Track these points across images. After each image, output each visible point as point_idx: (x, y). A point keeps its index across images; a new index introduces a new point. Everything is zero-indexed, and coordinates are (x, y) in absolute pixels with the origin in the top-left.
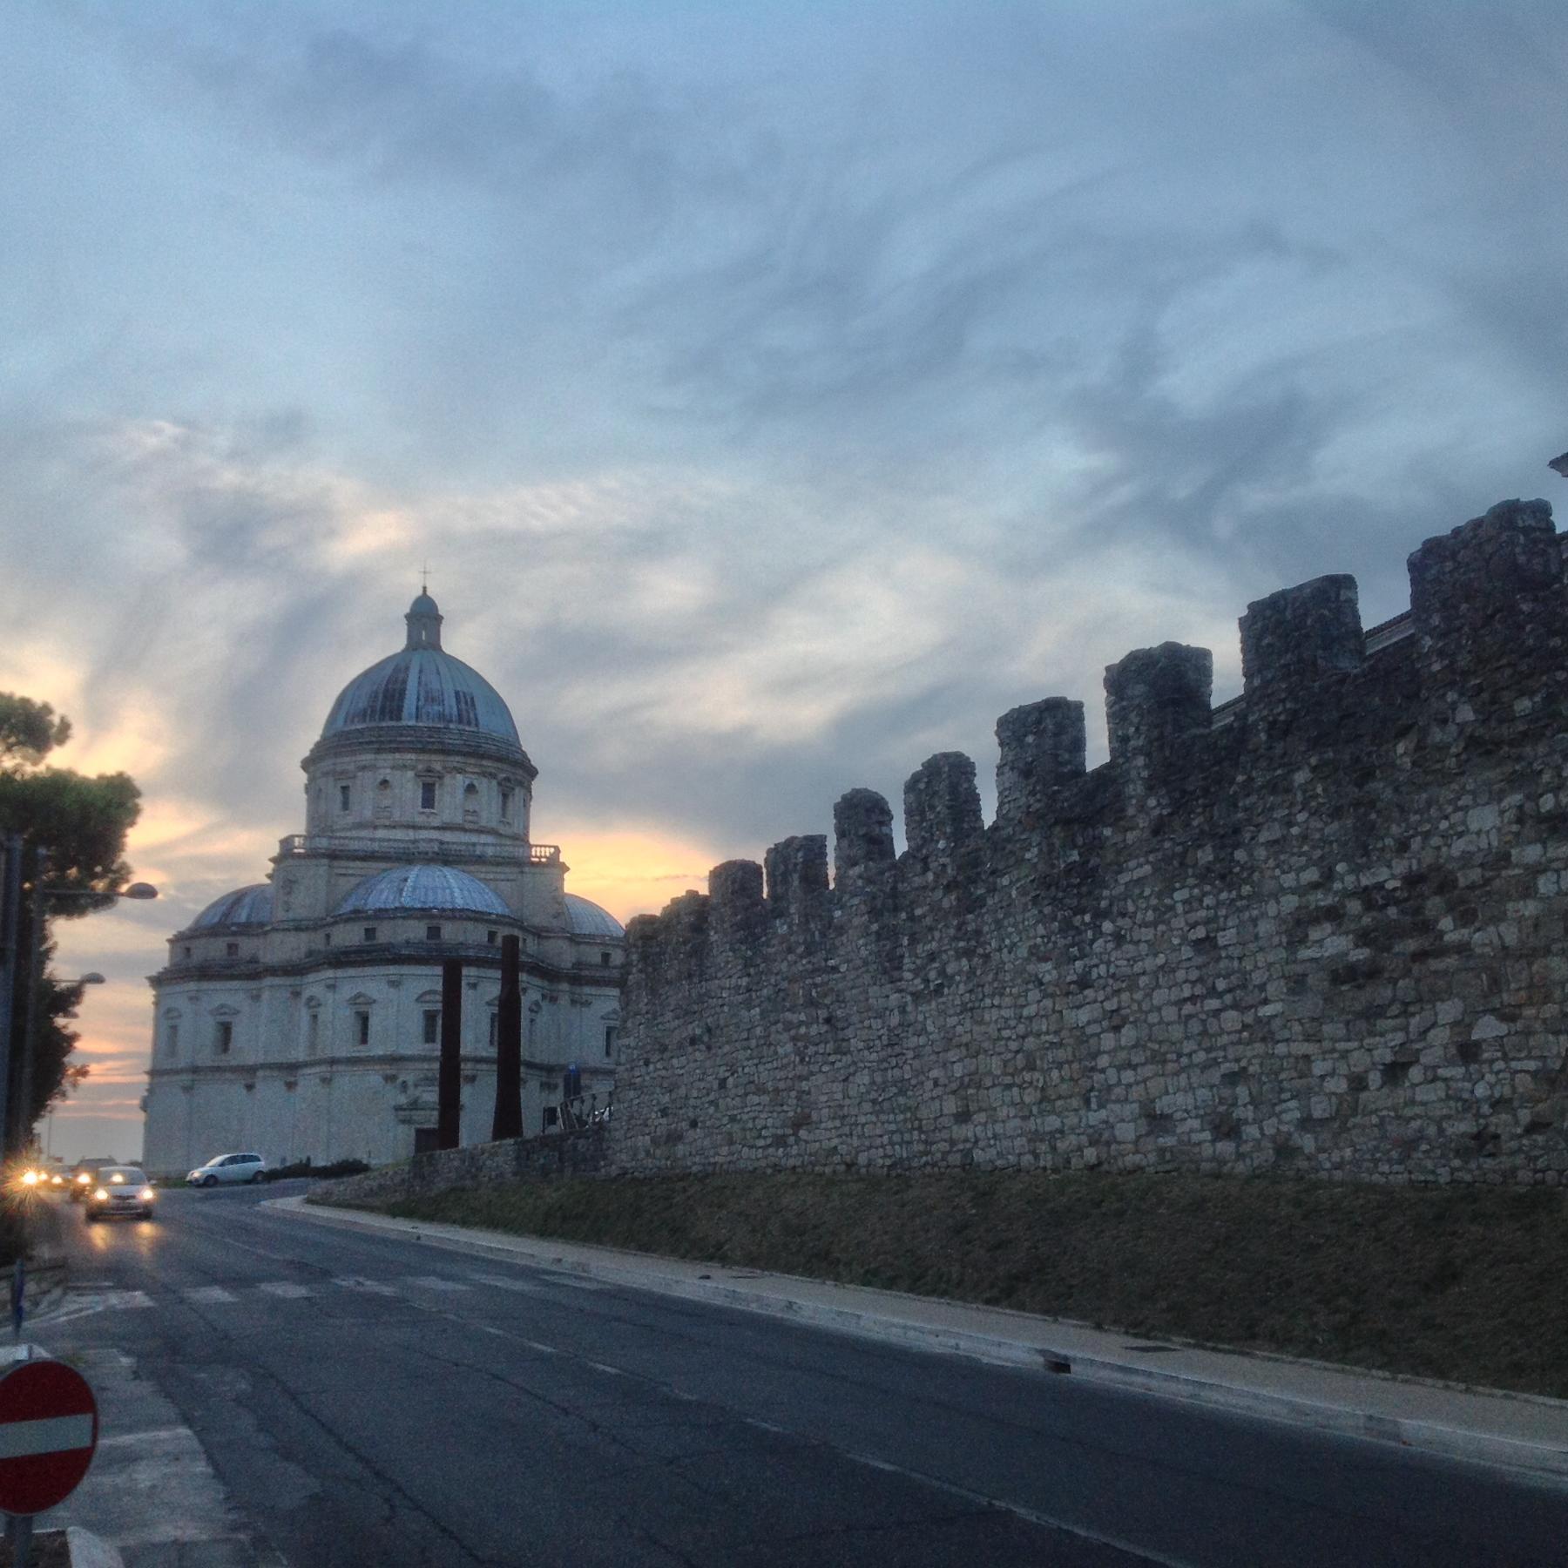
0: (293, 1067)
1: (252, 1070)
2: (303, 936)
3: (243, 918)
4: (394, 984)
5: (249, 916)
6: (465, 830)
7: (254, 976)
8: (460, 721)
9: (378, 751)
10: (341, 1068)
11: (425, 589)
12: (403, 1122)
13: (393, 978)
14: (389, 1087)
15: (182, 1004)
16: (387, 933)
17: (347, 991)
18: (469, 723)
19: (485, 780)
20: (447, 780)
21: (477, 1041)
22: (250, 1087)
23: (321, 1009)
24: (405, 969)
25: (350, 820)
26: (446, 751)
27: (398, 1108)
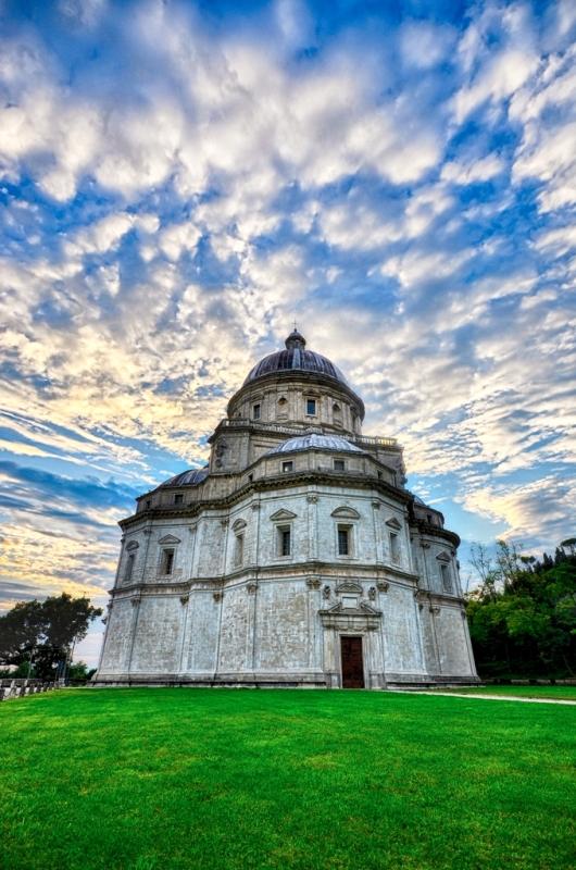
0: (220, 581)
1: (186, 586)
3: (188, 481)
4: (312, 500)
5: (192, 480)
9: (279, 382)
12: (329, 627)
13: (311, 495)
14: (313, 592)
16: (301, 465)
17: (270, 508)
20: (323, 399)
21: (385, 555)
22: (184, 601)
23: (246, 529)
24: (320, 489)
26: (320, 383)
27: (323, 614)
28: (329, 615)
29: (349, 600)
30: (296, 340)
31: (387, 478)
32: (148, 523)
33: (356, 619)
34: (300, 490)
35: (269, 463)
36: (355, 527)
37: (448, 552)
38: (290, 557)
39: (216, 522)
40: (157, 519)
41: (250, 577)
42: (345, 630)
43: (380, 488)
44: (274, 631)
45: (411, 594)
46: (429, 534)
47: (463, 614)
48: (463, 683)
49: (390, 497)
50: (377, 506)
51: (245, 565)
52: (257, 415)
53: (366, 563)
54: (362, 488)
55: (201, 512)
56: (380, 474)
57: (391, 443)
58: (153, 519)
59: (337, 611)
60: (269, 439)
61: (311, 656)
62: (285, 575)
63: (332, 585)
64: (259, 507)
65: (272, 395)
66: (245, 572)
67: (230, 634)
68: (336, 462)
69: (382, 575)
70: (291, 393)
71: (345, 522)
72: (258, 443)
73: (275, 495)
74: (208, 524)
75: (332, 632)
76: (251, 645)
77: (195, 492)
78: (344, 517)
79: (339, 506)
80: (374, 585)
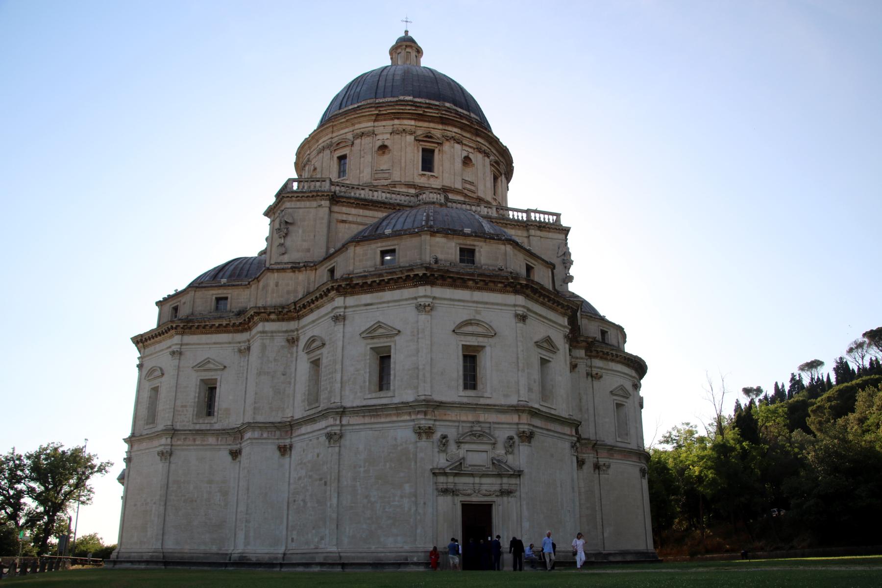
0: (290, 426)
1: (238, 433)
2: (301, 276)
6: (466, 196)
9: (377, 118)
10: (354, 420)
11: (406, 32)
12: (445, 491)
13: (422, 301)
14: (424, 443)
15: (165, 361)
19: (480, 156)
20: (447, 146)
21: (530, 390)
22: (235, 454)
23: (324, 351)
26: (443, 121)
28: (445, 474)
29: (476, 455)
30: (406, 47)
31: (542, 276)
32: (177, 339)
34: (408, 292)
35: (359, 250)
36: (488, 349)
37: (628, 386)
38: (390, 394)
39: (280, 341)
40: (194, 334)
41: (331, 421)
42: (469, 495)
43: (528, 292)
44: (367, 497)
45: (567, 445)
46: (602, 358)
47: (643, 472)
48: (642, 559)
49: (543, 304)
50: (523, 318)
51: (323, 406)
52: (342, 172)
53: (503, 401)
54: (503, 291)
55: (256, 324)
56: (529, 269)
57: (552, 219)
58: (183, 334)
59: (459, 469)
60: (361, 212)
61: (419, 531)
62: (383, 420)
63: (452, 433)
64: (344, 318)
65: (366, 140)
66: (324, 414)
67: (304, 501)
68: (462, 250)
69: (525, 418)
70: (397, 137)
71: (472, 341)
72: (344, 217)
73: (369, 301)
74: (267, 342)
75: (449, 498)
76: (334, 516)
77: (247, 292)
78: (472, 334)
79: (466, 317)
80: (512, 433)
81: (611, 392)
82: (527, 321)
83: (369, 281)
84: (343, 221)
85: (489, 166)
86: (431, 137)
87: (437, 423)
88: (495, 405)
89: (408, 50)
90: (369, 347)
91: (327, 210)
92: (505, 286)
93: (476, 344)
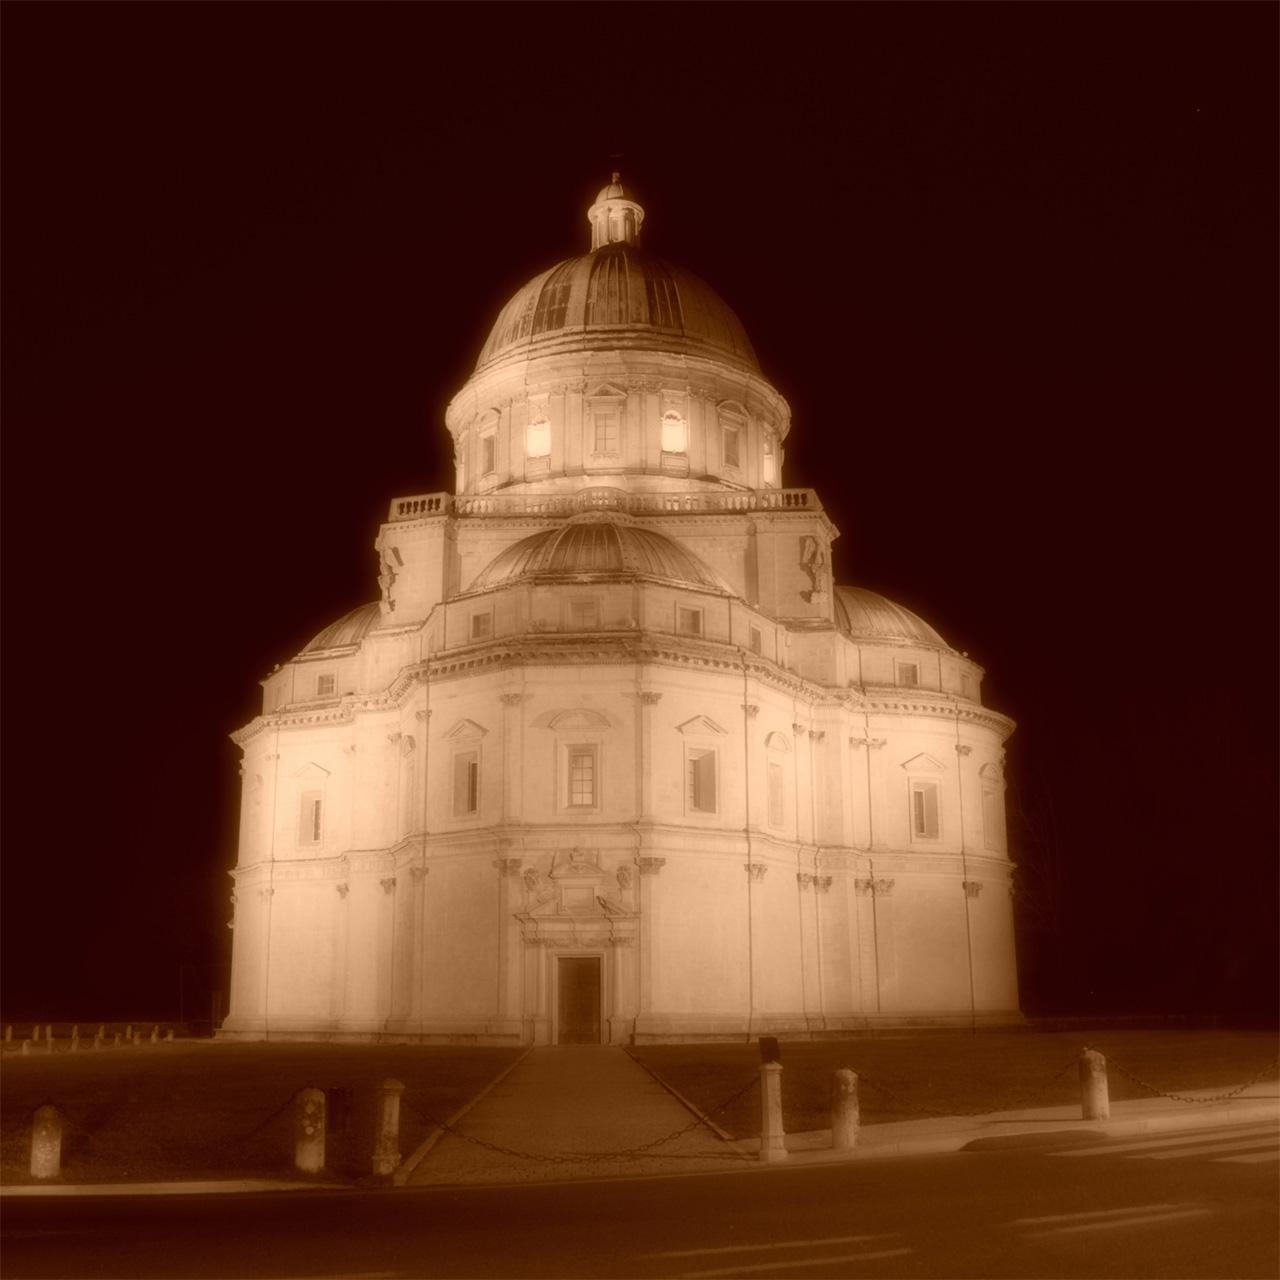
7: (347, 718)
8: (652, 321)
12: (536, 943)
18: (667, 325)
25: (494, 480)
33: (588, 927)
38: (475, 816)
42: (567, 946)
81: (903, 765)
82: (660, 701)
83: (449, 666)
84: (469, 554)
85: (714, 418)
86: (607, 393)
87: (527, 854)
88: (605, 825)
89: (612, 215)
90: (454, 753)
91: (441, 540)
92: (624, 656)
93: (584, 741)
